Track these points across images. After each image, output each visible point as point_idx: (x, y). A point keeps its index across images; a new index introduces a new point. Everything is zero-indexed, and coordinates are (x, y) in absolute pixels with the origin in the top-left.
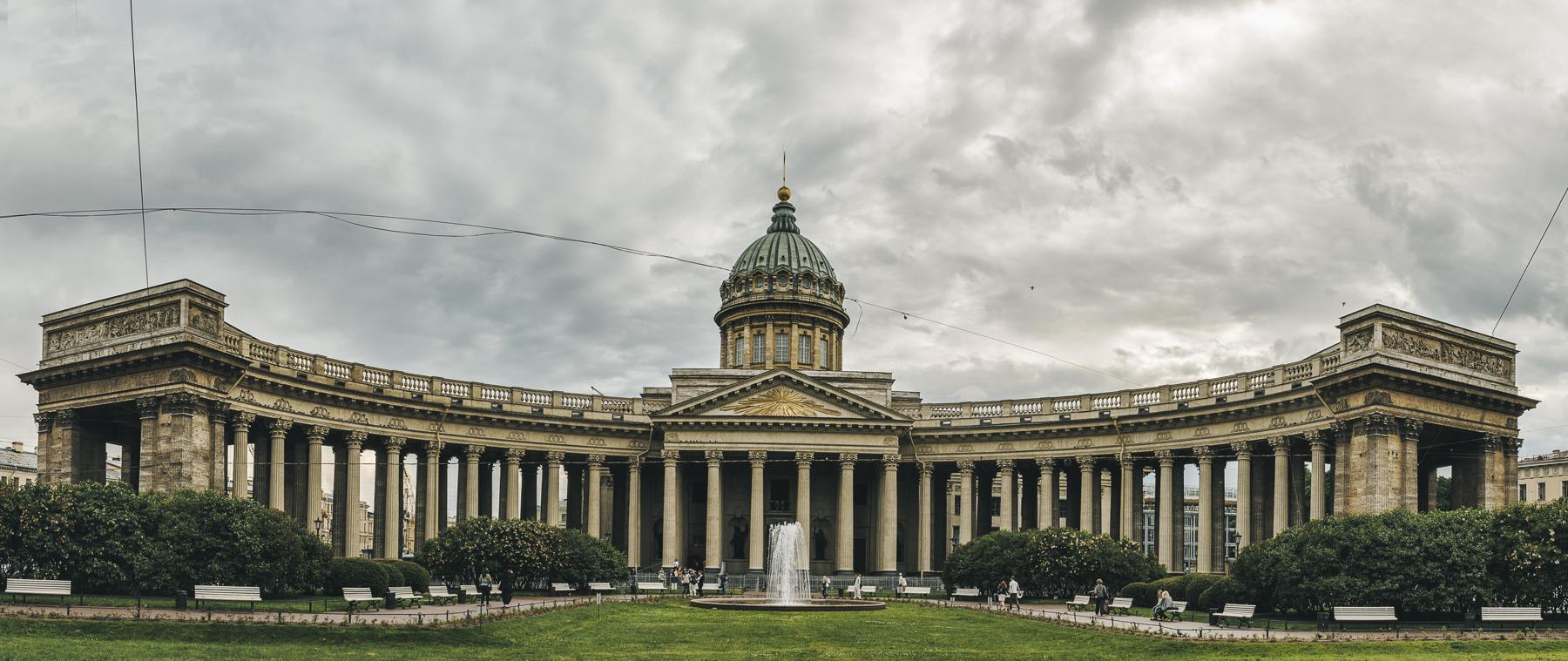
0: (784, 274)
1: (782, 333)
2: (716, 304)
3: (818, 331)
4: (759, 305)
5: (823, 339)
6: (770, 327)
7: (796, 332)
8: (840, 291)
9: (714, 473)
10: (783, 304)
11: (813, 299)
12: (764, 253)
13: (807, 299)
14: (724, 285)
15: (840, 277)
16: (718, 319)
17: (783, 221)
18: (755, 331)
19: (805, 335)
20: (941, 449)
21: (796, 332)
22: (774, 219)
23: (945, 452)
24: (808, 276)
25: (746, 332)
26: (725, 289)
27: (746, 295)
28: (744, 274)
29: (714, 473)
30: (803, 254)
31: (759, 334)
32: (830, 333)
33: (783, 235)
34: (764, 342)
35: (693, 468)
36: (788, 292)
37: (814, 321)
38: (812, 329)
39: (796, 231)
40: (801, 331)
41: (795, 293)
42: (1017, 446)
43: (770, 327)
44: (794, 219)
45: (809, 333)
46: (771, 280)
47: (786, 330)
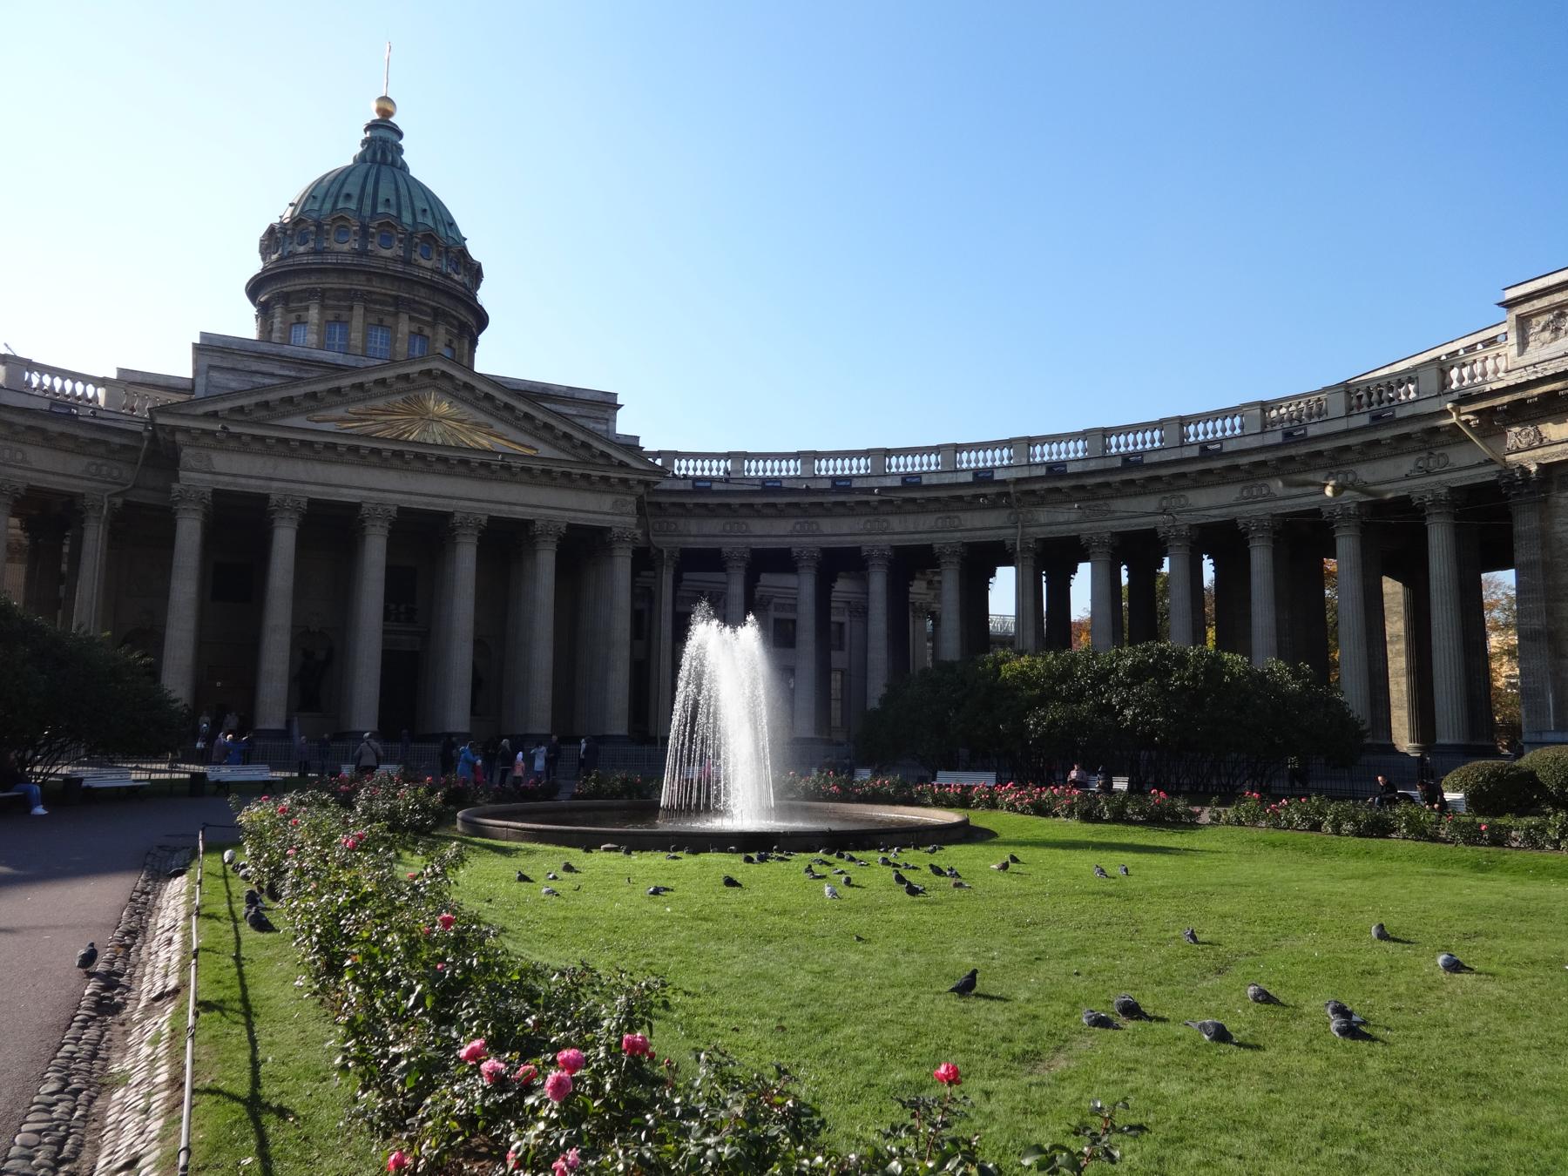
0: (388, 228)
1: (381, 323)
2: (255, 265)
3: (441, 330)
4: (342, 271)
5: (449, 345)
6: (359, 311)
7: (404, 327)
8: (476, 273)
9: (284, 539)
10: (382, 276)
11: (436, 278)
12: (352, 188)
13: (428, 275)
14: (271, 230)
15: (475, 251)
16: (255, 288)
17: (383, 142)
18: (330, 315)
19: (420, 333)
20: (693, 526)
21: (404, 327)
22: (363, 144)
23: (701, 532)
24: (430, 238)
25: (313, 314)
26: (273, 239)
27: (315, 252)
28: (314, 215)
29: (284, 539)
30: (420, 204)
31: (337, 320)
32: (460, 336)
33: (383, 168)
34: (346, 335)
35: (239, 524)
36: (394, 260)
37: (438, 314)
38: (433, 326)
39: (404, 167)
40: (414, 327)
41: (407, 262)
42: (827, 525)
43: (359, 311)
44: (400, 150)
45: (427, 331)
46: (364, 232)
47: (388, 320)
